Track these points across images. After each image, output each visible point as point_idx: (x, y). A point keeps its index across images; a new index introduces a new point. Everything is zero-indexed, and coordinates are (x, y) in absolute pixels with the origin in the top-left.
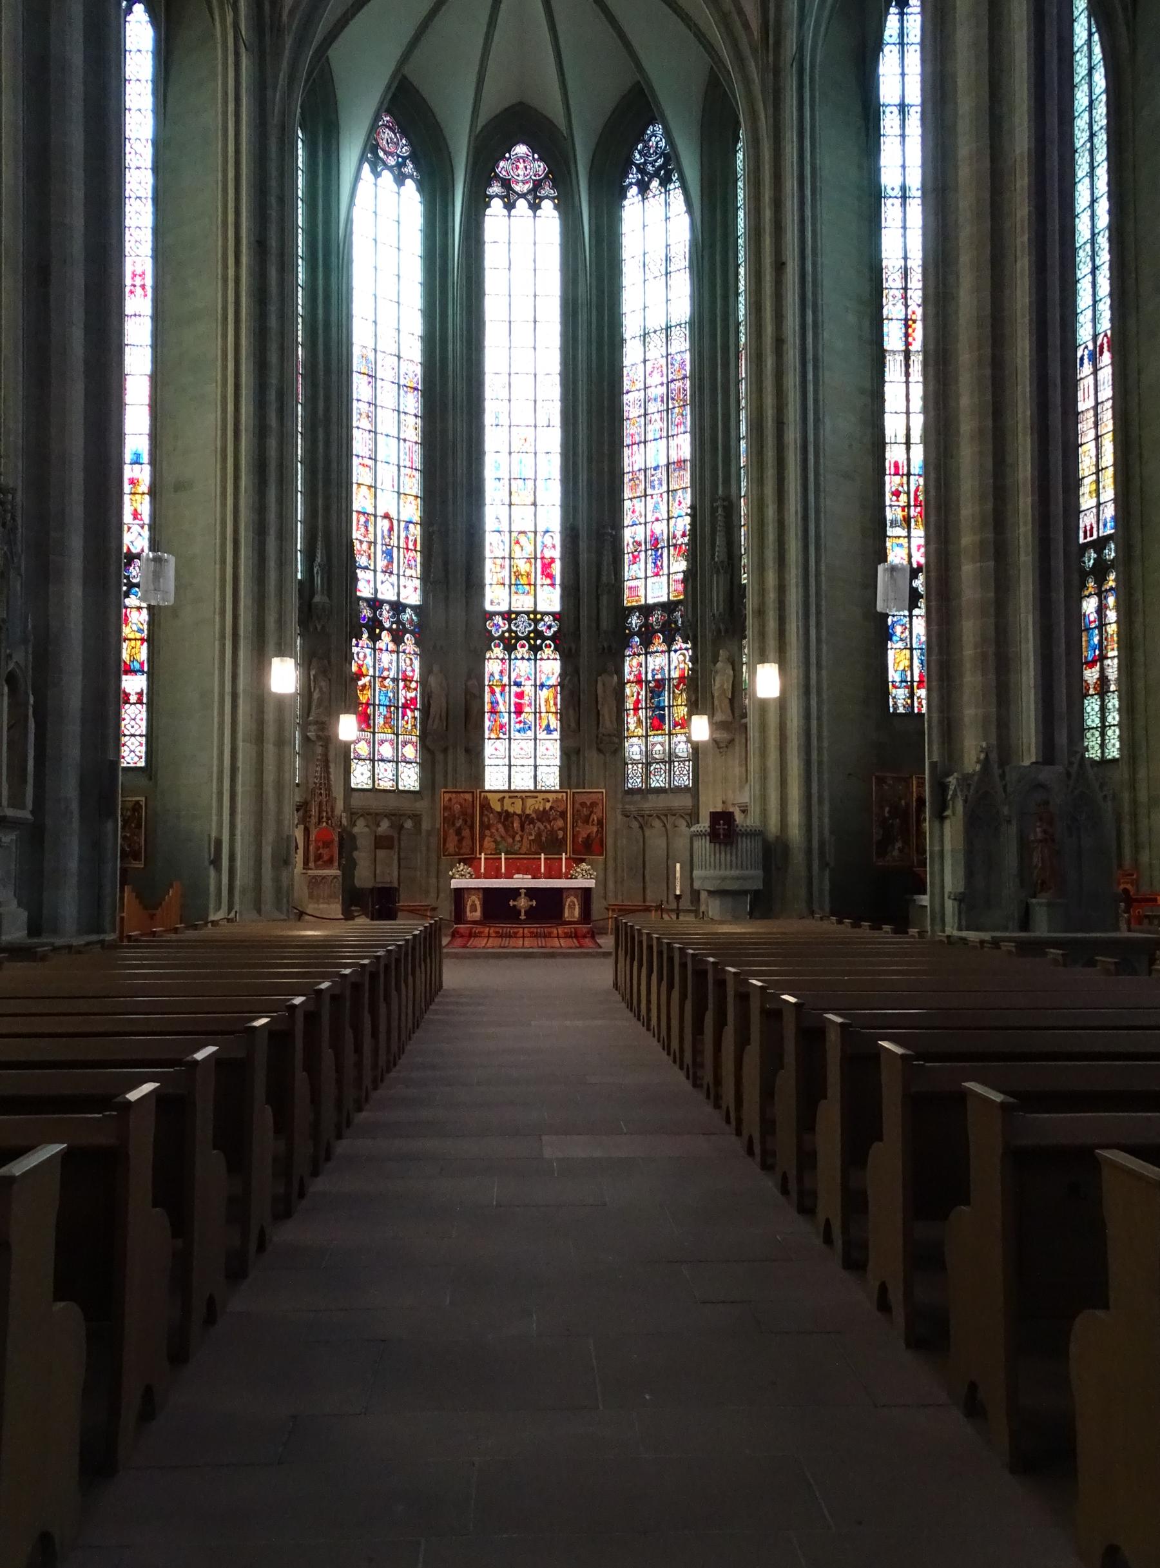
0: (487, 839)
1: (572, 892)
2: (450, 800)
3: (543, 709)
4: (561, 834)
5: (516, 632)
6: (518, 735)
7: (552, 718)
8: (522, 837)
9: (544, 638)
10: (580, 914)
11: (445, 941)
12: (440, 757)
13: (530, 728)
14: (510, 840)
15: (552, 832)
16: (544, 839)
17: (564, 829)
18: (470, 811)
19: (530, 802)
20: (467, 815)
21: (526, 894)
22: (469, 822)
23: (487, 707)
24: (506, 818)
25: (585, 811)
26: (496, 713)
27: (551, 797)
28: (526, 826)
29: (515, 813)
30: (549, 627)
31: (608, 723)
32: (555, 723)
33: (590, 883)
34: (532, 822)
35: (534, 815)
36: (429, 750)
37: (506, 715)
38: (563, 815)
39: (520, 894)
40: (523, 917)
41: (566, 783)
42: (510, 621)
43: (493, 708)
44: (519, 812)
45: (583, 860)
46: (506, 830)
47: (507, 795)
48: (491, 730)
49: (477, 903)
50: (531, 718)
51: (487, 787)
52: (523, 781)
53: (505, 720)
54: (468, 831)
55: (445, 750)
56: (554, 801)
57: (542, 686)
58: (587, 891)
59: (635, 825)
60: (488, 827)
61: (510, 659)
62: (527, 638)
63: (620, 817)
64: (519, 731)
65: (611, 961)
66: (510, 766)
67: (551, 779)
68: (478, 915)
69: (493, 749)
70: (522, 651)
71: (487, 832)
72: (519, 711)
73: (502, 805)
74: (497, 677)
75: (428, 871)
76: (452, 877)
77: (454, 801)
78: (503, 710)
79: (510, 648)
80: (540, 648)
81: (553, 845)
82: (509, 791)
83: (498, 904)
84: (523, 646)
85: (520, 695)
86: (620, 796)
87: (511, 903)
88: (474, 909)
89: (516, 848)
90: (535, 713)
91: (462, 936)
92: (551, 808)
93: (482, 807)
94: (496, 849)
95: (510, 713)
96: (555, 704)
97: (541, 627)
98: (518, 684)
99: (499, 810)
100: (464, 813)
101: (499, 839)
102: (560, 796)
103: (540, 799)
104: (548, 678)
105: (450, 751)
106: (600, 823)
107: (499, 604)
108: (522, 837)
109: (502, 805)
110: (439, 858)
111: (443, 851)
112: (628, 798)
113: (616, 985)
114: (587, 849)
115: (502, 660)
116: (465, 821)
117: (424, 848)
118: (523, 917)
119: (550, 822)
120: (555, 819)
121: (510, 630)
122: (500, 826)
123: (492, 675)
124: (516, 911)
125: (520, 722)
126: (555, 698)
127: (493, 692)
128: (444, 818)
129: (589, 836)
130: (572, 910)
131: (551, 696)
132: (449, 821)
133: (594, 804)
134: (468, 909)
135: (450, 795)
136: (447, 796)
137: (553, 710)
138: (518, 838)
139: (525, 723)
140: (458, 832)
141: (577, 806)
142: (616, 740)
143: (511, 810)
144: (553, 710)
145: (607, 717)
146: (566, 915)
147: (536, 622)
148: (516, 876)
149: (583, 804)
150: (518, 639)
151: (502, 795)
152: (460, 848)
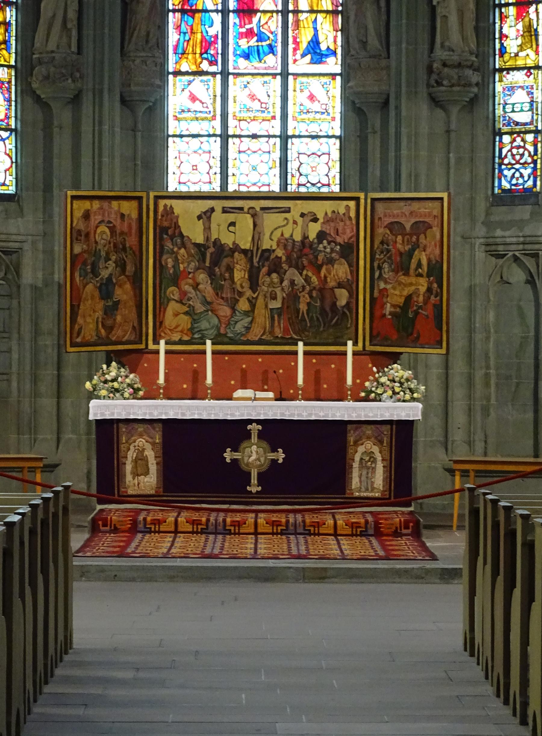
0: (172, 307)
1: (369, 430)
2: (87, 216)
4: (343, 297)
6: (243, 63)
8: (252, 303)
10: (388, 480)
11: (77, 540)
12: (63, 116)
13: (272, 49)
14: (225, 311)
15: (323, 292)
16: (303, 307)
17: (351, 286)
18: (132, 241)
19: (271, 221)
20: (126, 250)
21: (261, 435)
22: (130, 269)
24: (216, 262)
25: (400, 244)
27: (321, 209)
28: (263, 278)
29: (236, 248)
31: (455, 37)
33: (411, 411)
34: (276, 267)
35: (280, 253)
36: (38, 99)
37: (217, 18)
38: (349, 251)
39: (248, 435)
40: (254, 488)
41: (354, 180)
44: (246, 244)
45: (395, 358)
46: (218, 289)
47: (218, 205)
49: (150, 454)
51: (173, 186)
52: (253, 172)
53: (216, 29)
54: (128, 286)
55: (76, 100)
56: (328, 221)
58: (403, 430)
59: (517, 276)
60: (176, 280)
63: (480, 255)
64: (247, 56)
65: (459, 589)
66: (225, 137)
67: (320, 167)
68: (149, 482)
71: (173, 292)
73: (207, 229)
75: (35, 380)
76: (92, 395)
77: (95, 219)
81: (325, 321)
82: (223, 195)
83: (197, 458)
86: (481, 205)
87: (228, 455)
88: (140, 467)
89: (239, 327)
90: (285, 12)
91: (115, 530)
92: (321, 236)
93: (161, 232)
94: (192, 330)
95: (225, 12)
99: (200, 239)
100: (120, 248)
101: (200, 308)
102: (341, 207)
103: (295, 214)
105: (87, 108)
106: (435, 271)
108: (252, 303)
109: (207, 229)
110: (60, 347)
111: (69, 334)
112: (501, 213)
113: (470, 645)
114: (406, 330)
116: (121, 265)
117: (27, 328)
118: (254, 488)
119: (319, 268)
120: (331, 261)
122: (202, 277)
124: (238, 475)
125: (250, 33)
128: (74, 258)
129: (409, 299)
130: (368, 473)
132: (84, 264)
133: (421, 227)
134: (129, 467)
135: (87, 204)
136: (81, 207)
138: (243, 305)
140: (106, 290)
141: (380, 230)
142: (475, 78)
143: (227, 240)
145: (453, 19)
146: (355, 482)
148: (239, 393)
149: (395, 227)
151: (210, 203)
152: (110, 329)
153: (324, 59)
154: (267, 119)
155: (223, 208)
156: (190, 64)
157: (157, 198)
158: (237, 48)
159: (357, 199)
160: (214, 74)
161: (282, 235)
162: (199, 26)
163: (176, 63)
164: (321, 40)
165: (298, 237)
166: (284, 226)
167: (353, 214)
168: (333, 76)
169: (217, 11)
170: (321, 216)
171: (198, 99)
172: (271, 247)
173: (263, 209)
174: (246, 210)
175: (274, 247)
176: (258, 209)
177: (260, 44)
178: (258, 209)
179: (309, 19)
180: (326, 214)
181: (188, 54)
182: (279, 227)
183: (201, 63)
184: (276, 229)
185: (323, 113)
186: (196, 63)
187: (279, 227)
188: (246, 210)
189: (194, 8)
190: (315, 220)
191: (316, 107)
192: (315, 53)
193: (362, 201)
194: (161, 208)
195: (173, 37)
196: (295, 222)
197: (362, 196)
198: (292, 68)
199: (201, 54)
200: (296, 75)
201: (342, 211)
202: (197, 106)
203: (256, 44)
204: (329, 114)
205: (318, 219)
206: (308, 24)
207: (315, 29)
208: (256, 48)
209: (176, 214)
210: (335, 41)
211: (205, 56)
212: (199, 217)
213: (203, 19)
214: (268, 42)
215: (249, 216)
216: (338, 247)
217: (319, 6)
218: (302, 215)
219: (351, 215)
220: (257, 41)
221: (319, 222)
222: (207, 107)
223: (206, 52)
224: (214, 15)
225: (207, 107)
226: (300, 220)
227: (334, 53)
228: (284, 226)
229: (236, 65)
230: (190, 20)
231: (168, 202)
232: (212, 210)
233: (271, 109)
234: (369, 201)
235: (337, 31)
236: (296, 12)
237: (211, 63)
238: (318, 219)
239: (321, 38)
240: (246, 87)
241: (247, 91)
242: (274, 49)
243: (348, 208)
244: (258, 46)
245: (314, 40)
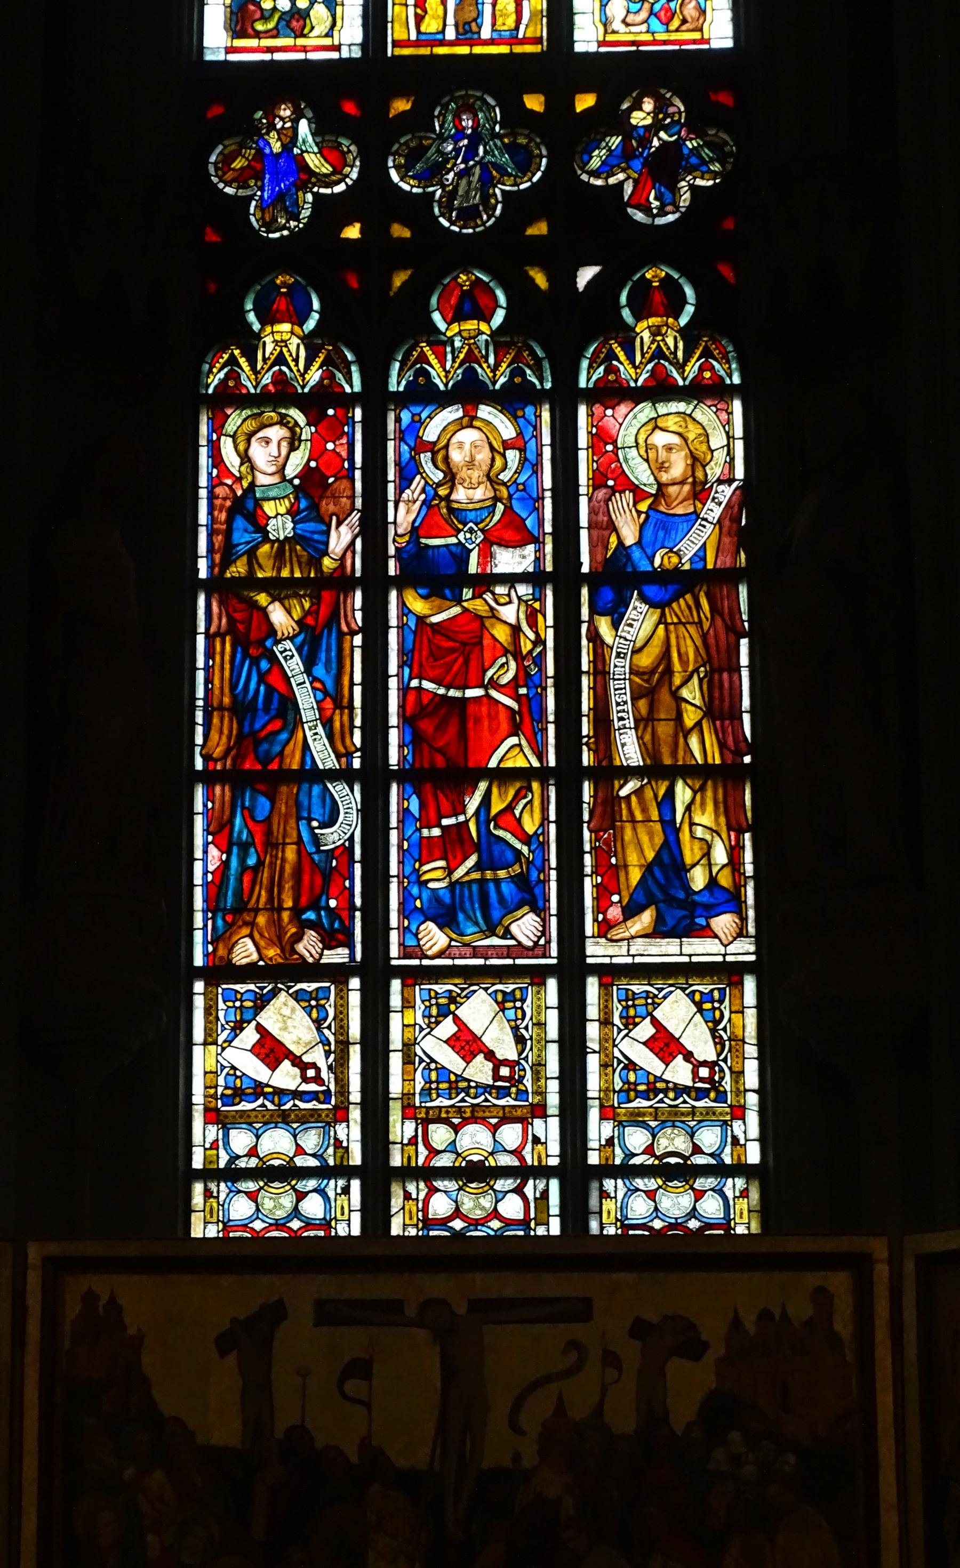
3: (630, 750)
5: (416, 210)
6: (434, 937)
7: (702, 822)
9: (625, 247)
23: (206, 741)
26: (273, 779)
30: (665, 168)
32: (711, 847)
37: (348, 798)
42: (375, 142)
43: (246, 741)
44: (412, 1449)
48: (232, 911)
50: (536, 814)
53: (346, 828)
57: (618, 581)
61: (376, 400)
62: (502, 252)
64: (445, 916)
69: (249, 1047)
70: (463, 338)
72: (445, 767)
74: (281, 527)
78: (323, 756)
79: (373, 321)
80: (596, 321)
84: (472, 306)
85: (454, 651)
90: (567, 776)
92: (718, 1411)
95: (374, 780)
96: (720, 710)
97: (598, 165)
98: (440, 574)
104: (661, 524)
107: (296, 20)
115: (317, 403)
121: (372, 199)
123: (246, 506)
125: (454, 845)
126: (717, 665)
127: (251, 637)
131: (689, 645)
137: (702, 748)
139: (491, 854)
144: (702, 748)
147: (568, 137)
150: (436, 256)
153: (701, 921)
154: (519, 1113)
155: (320, 1304)
156: (262, 943)
157: (57, 1268)
158: (415, 891)
159: (859, 1265)
160: (339, 974)
161: (560, 1408)
162: (292, 822)
163: (214, 942)
164: (688, 860)
165: (624, 1420)
166: (568, 1373)
167: (843, 1326)
168: (730, 973)
169: (346, 775)
170: (713, 1331)
171: (289, 1055)
172: (517, 1458)
173: (476, 1305)
174: (411, 1311)
175: (530, 1460)
176: (461, 1308)
177: (489, 874)
178: (461, 1308)
179: (649, 794)
180: (736, 1323)
181: (256, 911)
182: (546, 1380)
183: (298, 937)
184: (535, 1386)
185: (701, 1094)
186: (280, 938)
187: (546, 1380)
188: (411, 1311)
189: (274, 766)
190: (694, 1348)
191: (680, 1072)
192: (671, 901)
193: (882, 1271)
194: (73, 1309)
195: (206, 859)
196: (611, 1359)
197: (879, 1248)
198: (597, 951)
199: (297, 911)
200: (610, 973)
201: (801, 1309)
202: (286, 1077)
203: (476, 875)
204: (721, 1096)
205: (706, 1345)
206: (644, 810)
207: (670, 827)
208: (475, 888)
209: (132, 1331)
210: (735, 861)
211: (310, 915)
212: (224, 1344)
213: (303, 798)
214: (517, 869)
215: (422, 1334)
216: (792, 1459)
217: (681, 753)
218: (639, 1329)
219: (838, 1327)
220: (478, 867)
221: (709, 1358)
222: (318, 1080)
223: (314, 905)
224: (338, 790)
225: (318, 1080)
226: (631, 1353)
227: (734, 903)
228: (568, 1373)
229: (411, 942)
230: (263, 806)
231: (102, 1285)
232: (276, 1312)
233: (528, 1082)
234: (909, 1267)
235: (740, 832)
236: (608, 773)
237: (329, 942)
238: (706, 1345)
239: (690, 853)
240: (444, 1013)
241: (447, 1028)
242: (537, 891)
243: (822, 1296)
244: (482, 882)
245: (666, 858)
